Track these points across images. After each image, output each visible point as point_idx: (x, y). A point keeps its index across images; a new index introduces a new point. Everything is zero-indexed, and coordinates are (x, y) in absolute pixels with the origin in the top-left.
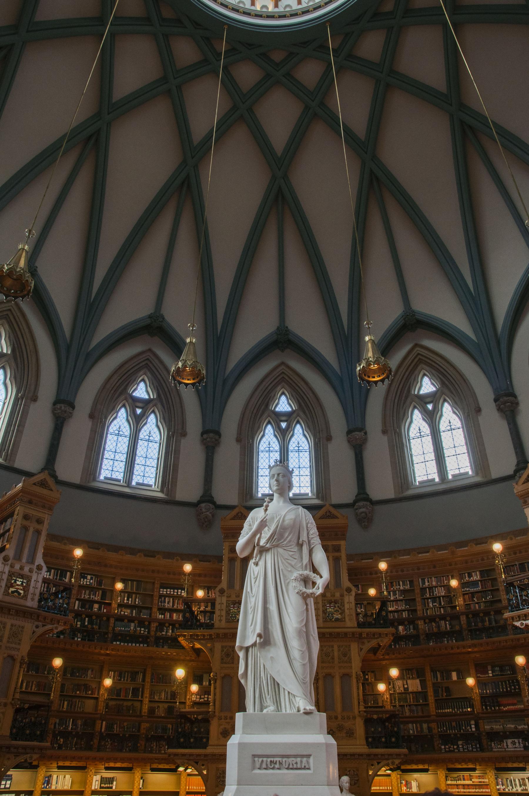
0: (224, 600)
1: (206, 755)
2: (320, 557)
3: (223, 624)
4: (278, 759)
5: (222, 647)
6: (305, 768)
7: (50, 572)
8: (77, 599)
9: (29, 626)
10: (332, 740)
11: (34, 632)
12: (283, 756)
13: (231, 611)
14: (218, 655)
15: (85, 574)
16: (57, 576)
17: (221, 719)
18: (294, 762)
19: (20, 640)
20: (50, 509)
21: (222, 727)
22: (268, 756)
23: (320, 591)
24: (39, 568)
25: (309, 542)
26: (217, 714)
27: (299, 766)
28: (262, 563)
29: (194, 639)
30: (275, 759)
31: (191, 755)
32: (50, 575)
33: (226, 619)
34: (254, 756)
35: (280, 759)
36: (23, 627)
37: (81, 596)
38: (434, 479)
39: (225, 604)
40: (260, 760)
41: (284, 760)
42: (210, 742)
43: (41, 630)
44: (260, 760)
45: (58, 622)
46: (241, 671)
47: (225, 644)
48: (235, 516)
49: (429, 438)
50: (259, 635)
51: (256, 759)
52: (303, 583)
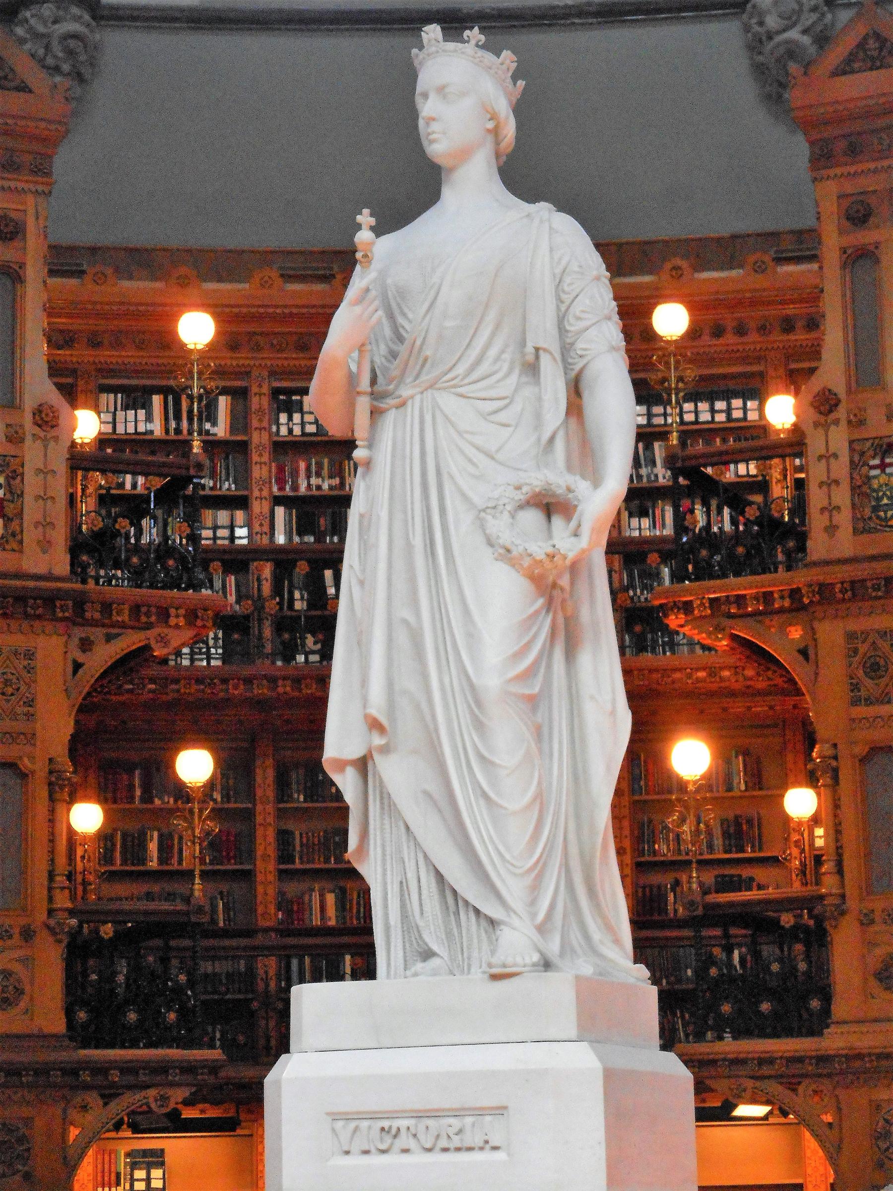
0: (839, 438)
1: (822, 1059)
3: (845, 543)
4: (403, 1123)
5: (851, 636)
6: (487, 1145)
7: (147, 405)
8: (278, 501)
9: (51, 648)
11: (77, 666)
12: (419, 1115)
13: (875, 484)
14: (834, 669)
15: (289, 392)
16: (178, 417)
17: (872, 922)
18: (451, 1131)
19: (30, 703)
20: (41, 169)
21: (879, 952)
22: (373, 1116)
24: (47, 421)
25: (566, 349)
26: (852, 904)
29: (730, 616)
30: (396, 1124)
31: (765, 1061)
32: (149, 418)
33: (855, 519)
34: (335, 1117)
35: (410, 1122)
36: (30, 655)
37: (295, 487)
39: (845, 458)
42: (840, 1009)
43: (104, 654)
44: (353, 1125)
45: (164, 614)
47: (853, 625)
48: (851, 58)
51: (340, 1124)
52: (532, 517)
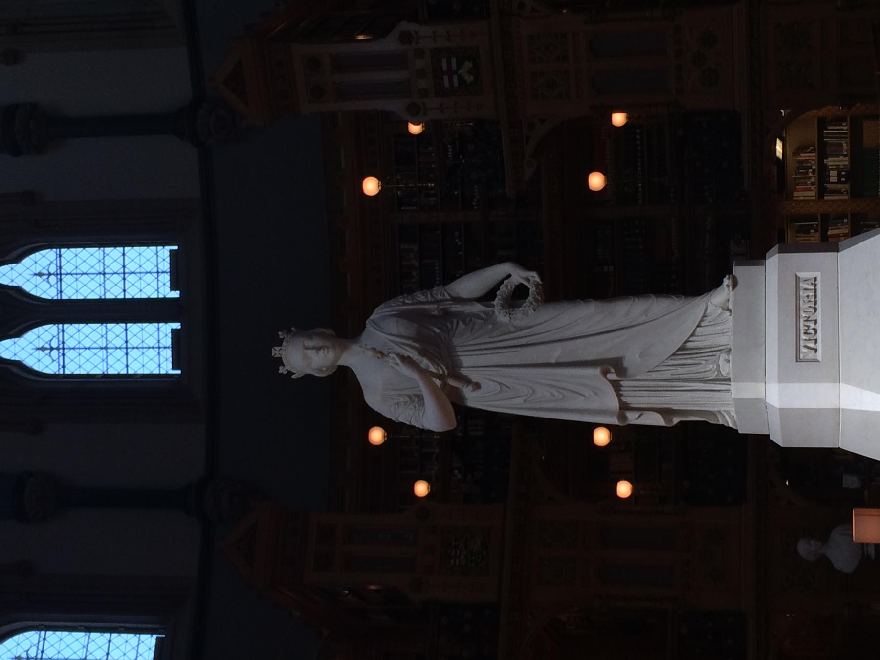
2: (470, 285)
10: (774, 261)
12: (798, 316)
18: (806, 299)
23: (534, 276)
27: (811, 294)
28: (474, 376)
30: (802, 328)
34: (798, 360)
35: (802, 320)
38: (173, 331)
40: (804, 350)
41: (803, 315)
46: (658, 420)
49: (71, 329)
50: (605, 373)
